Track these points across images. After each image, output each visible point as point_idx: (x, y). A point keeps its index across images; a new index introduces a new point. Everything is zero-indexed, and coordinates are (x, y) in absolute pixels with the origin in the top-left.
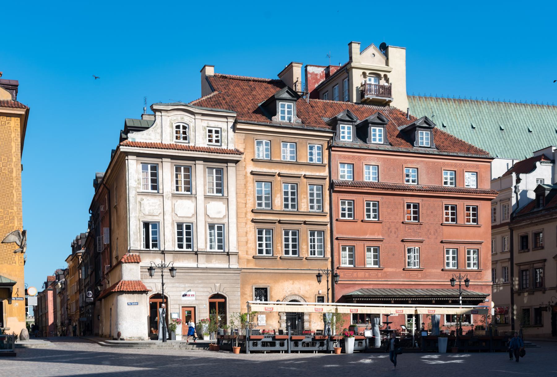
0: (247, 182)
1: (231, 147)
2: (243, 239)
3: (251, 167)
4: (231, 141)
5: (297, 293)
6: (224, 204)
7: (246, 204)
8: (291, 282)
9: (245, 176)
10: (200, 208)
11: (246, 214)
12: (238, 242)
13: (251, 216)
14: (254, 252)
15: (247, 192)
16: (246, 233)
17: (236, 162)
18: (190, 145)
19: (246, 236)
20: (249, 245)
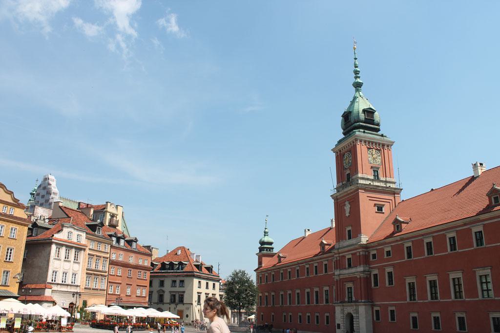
2: (82, 280)
3: (88, 251)
4: (83, 240)
10: (71, 267)
12: (81, 281)
14: (84, 286)
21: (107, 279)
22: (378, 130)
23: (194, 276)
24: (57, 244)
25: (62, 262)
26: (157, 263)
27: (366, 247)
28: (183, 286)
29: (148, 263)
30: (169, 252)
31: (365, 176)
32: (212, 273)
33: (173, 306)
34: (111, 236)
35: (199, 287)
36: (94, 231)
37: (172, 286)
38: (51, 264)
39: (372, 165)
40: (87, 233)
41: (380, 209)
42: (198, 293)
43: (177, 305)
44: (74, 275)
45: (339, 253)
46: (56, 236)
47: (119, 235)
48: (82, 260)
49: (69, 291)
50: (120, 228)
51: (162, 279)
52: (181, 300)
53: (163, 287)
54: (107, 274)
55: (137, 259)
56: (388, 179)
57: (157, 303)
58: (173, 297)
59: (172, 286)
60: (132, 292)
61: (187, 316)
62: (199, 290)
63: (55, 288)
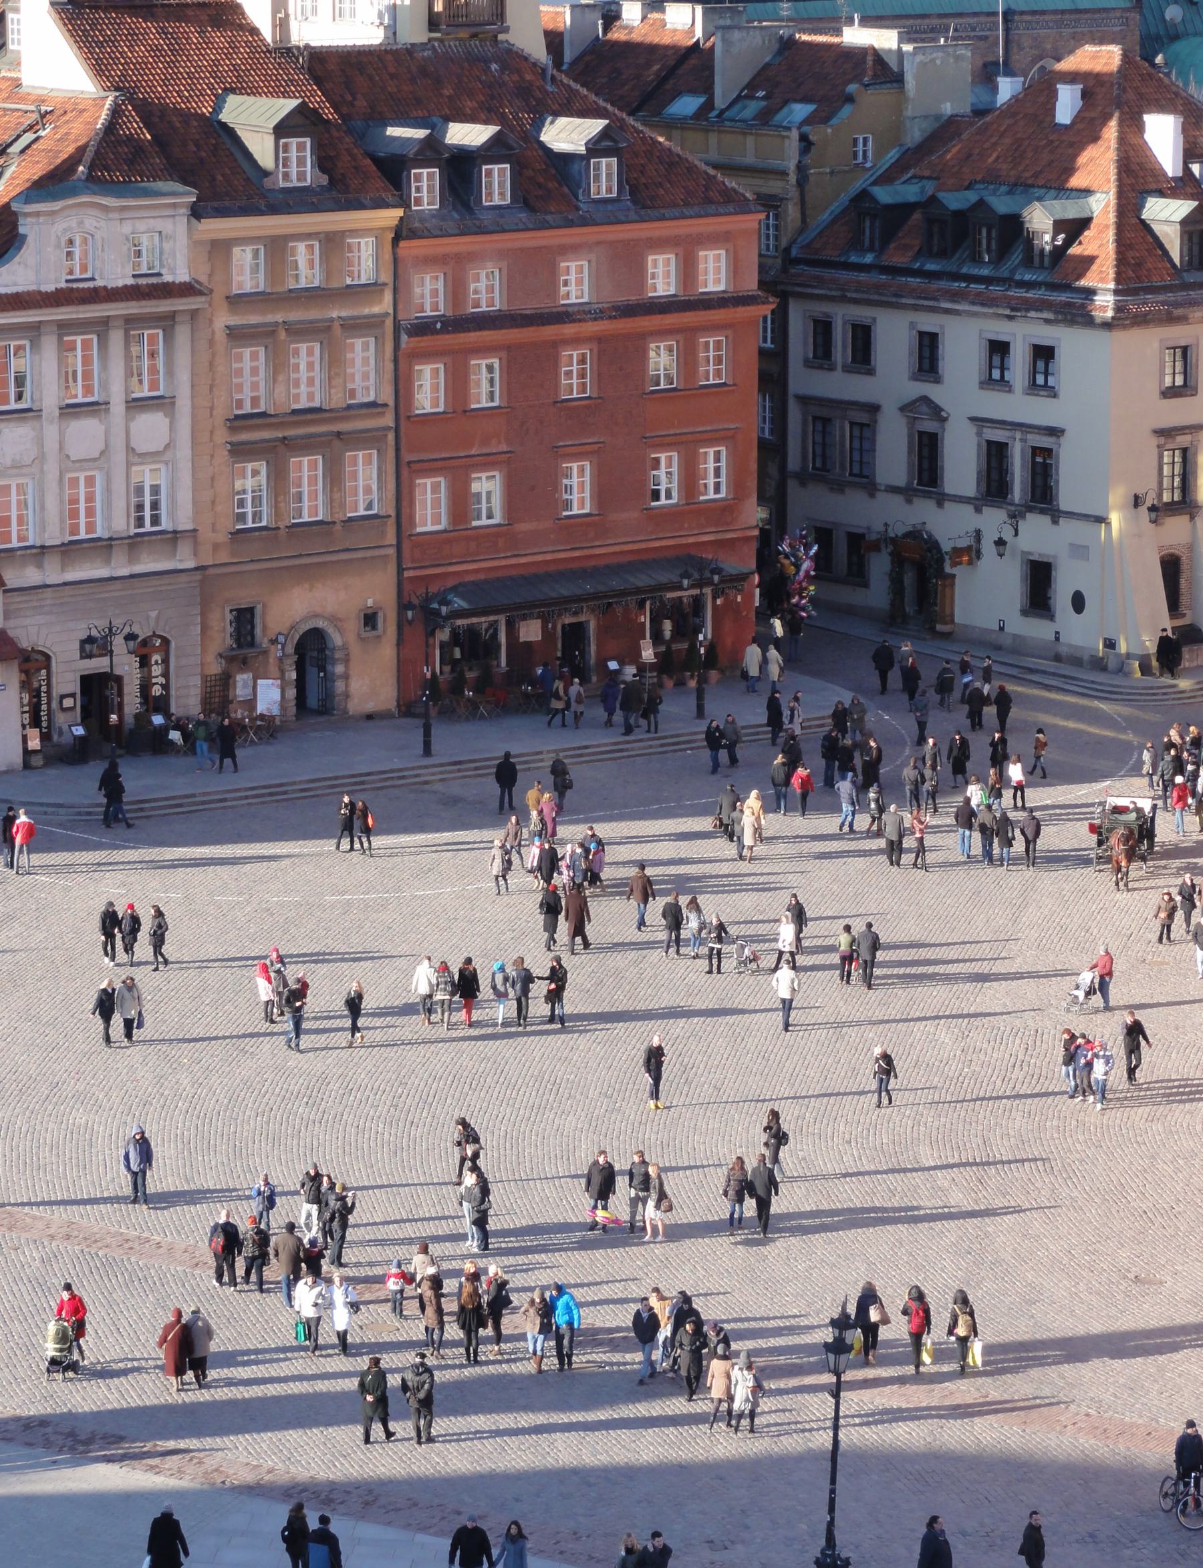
0: (214, 355)
1: (182, 275)
3: (223, 319)
5: (318, 610)
6: (165, 415)
7: (212, 409)
8: (307, 586)
9: (211, 342)
11: (212, 432)
13: (222, 436)
14: (228, 525)
15: (213, 380)
16: (213, 479)
17: (194, 314)
18: (100, 283)
19: (212, 487)
20: (219, 508)
21: (391, 453)
25: (51, 431)
28: (1052, 392)
29: (735, 269)
33: (993, 521)
35: (1171, 393)
37: (988, 382)
40: (196, 213)
42: (1165, 433)
43: (1015, 517)
48: (184, 377)
49: (124, 572)
51: (928, 322)
52: (1043, 495)
53: (938, 380)
54: (388, 420)
55: (630, 261)
57: (908, 493)
58: (996, 454)
59: (988, 382)
60: (603, 493)
61: (1078, 602)
63: (31, 576)
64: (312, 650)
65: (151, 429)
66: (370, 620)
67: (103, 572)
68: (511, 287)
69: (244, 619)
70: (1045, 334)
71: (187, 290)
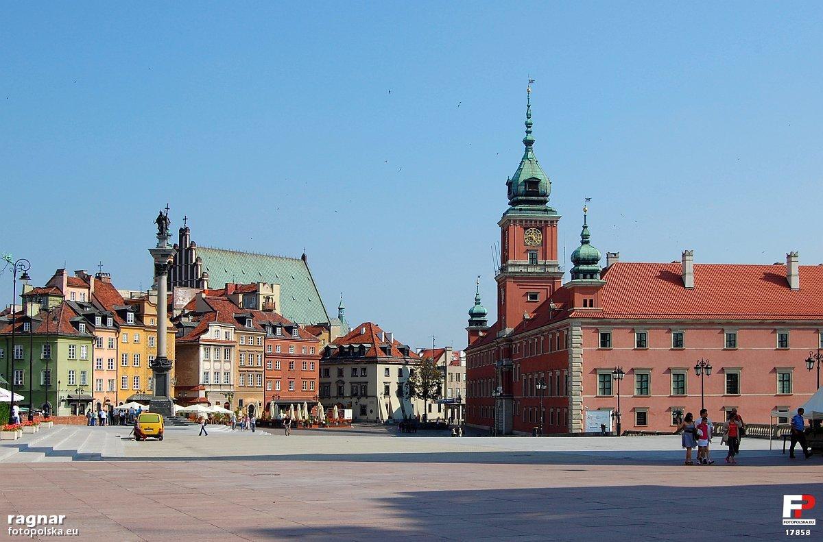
4: (232, 337)
22: (545, 202)
23: (377, 363)
24: (204, 345)
26: (335, 347)
27: (509, 339)
28: (366, 376)
30: (352, 330)
31: (518, 261)
32: (408, 356)
33: (354, 400)
34: (264, 326)
36: (244, 324)
38: (201, 366)
39: (528, 248)
40: (235, 329)
41: (534, 297)
44: (227, 373)
45: (498, 343)
46: (203, 337)
47: (275, 324)
50: (278, 311)
51: (341, 367)
53: (343, 376)
55: (301, 348)
56: (548, 262)
57: (337, 397)
61: (371, 411)
62: (387, 379)
64: (252, 408)
65: (227, 366)
66: (260, 404)
67: (220, 390)
68: (283, 349)
69: (241, 401)
70: (364, 366)
71: (234, 342)
